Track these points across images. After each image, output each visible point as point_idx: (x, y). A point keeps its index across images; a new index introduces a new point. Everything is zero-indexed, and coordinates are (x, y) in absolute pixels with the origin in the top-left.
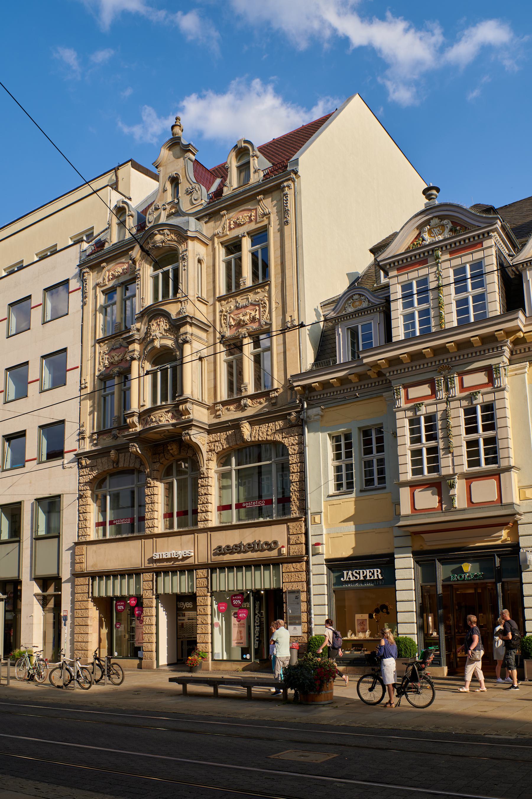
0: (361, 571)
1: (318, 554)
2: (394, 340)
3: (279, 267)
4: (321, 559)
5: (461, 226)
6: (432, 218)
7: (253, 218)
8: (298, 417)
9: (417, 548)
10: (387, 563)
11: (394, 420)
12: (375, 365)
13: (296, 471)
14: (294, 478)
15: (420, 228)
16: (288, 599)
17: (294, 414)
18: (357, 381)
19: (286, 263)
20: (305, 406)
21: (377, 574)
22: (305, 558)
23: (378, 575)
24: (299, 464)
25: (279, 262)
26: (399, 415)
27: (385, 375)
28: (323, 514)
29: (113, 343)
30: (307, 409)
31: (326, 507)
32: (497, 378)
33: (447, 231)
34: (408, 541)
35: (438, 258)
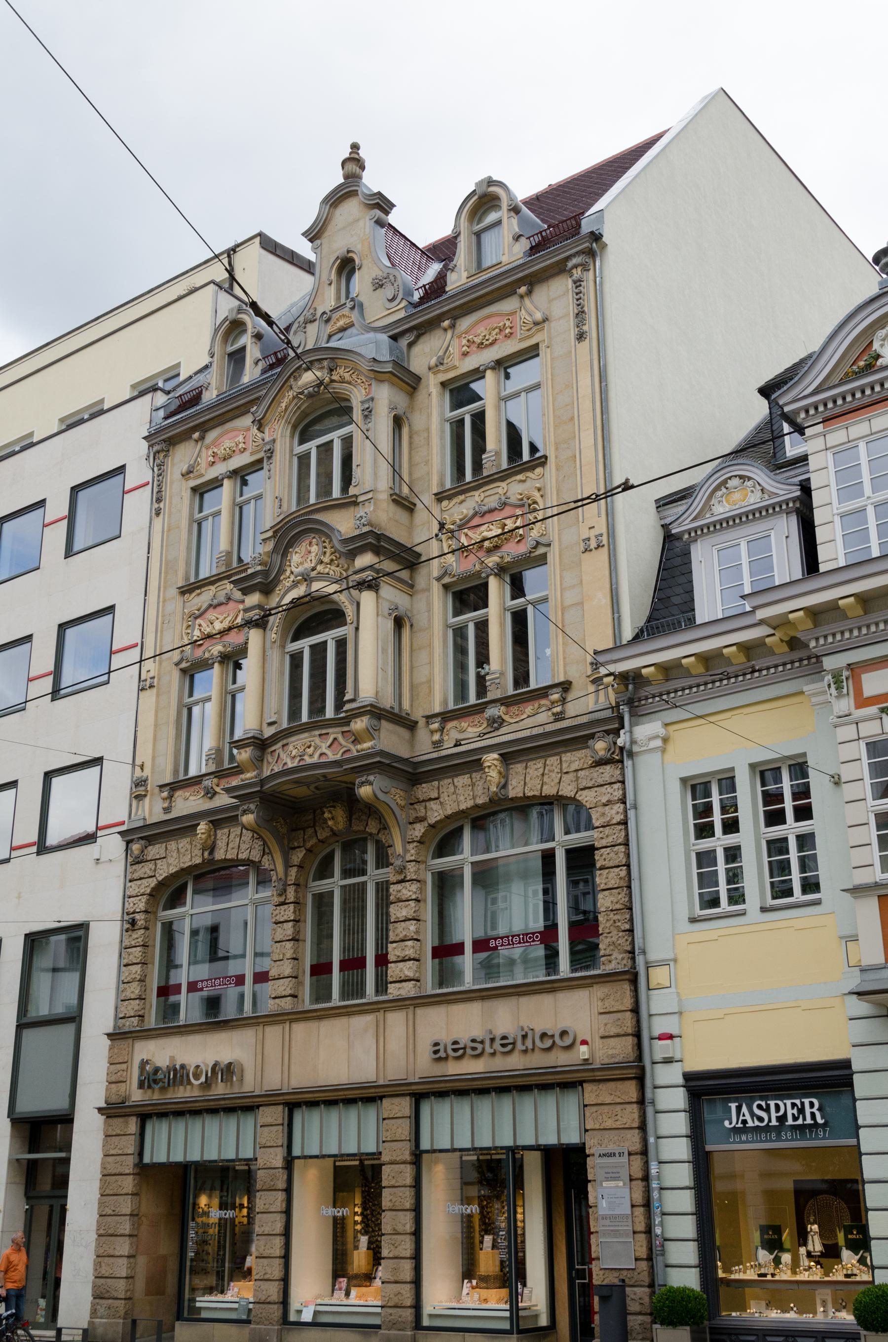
0: (772, 1103)
2: (822, 568)
23: (813, 1115)
29: (211, 593)
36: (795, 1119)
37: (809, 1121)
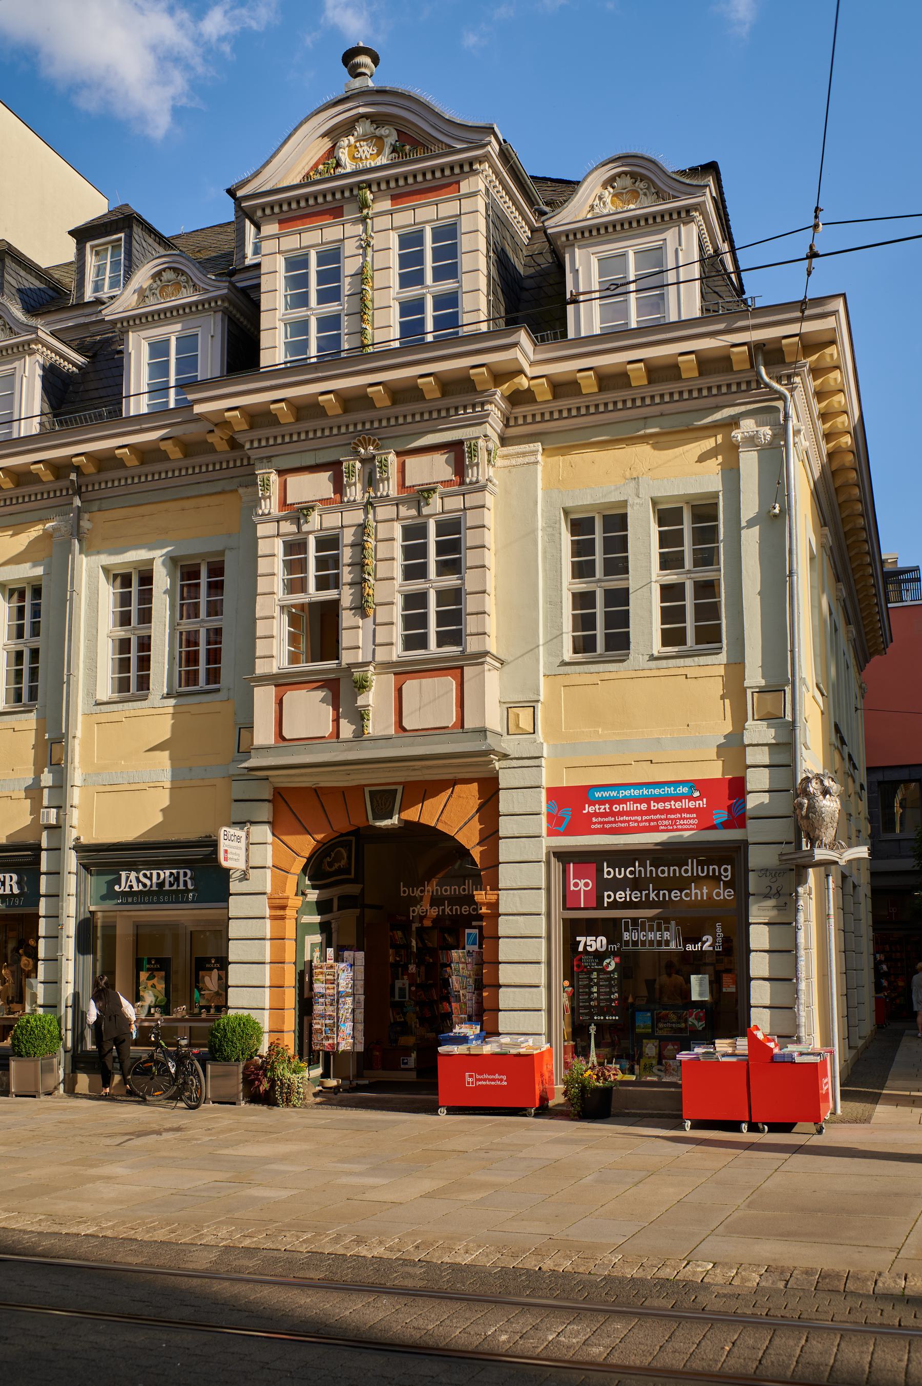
0: (155, 873)
12: (219, 422)
27: (242, 446)
36: (171, 885)
37: (182, 887)
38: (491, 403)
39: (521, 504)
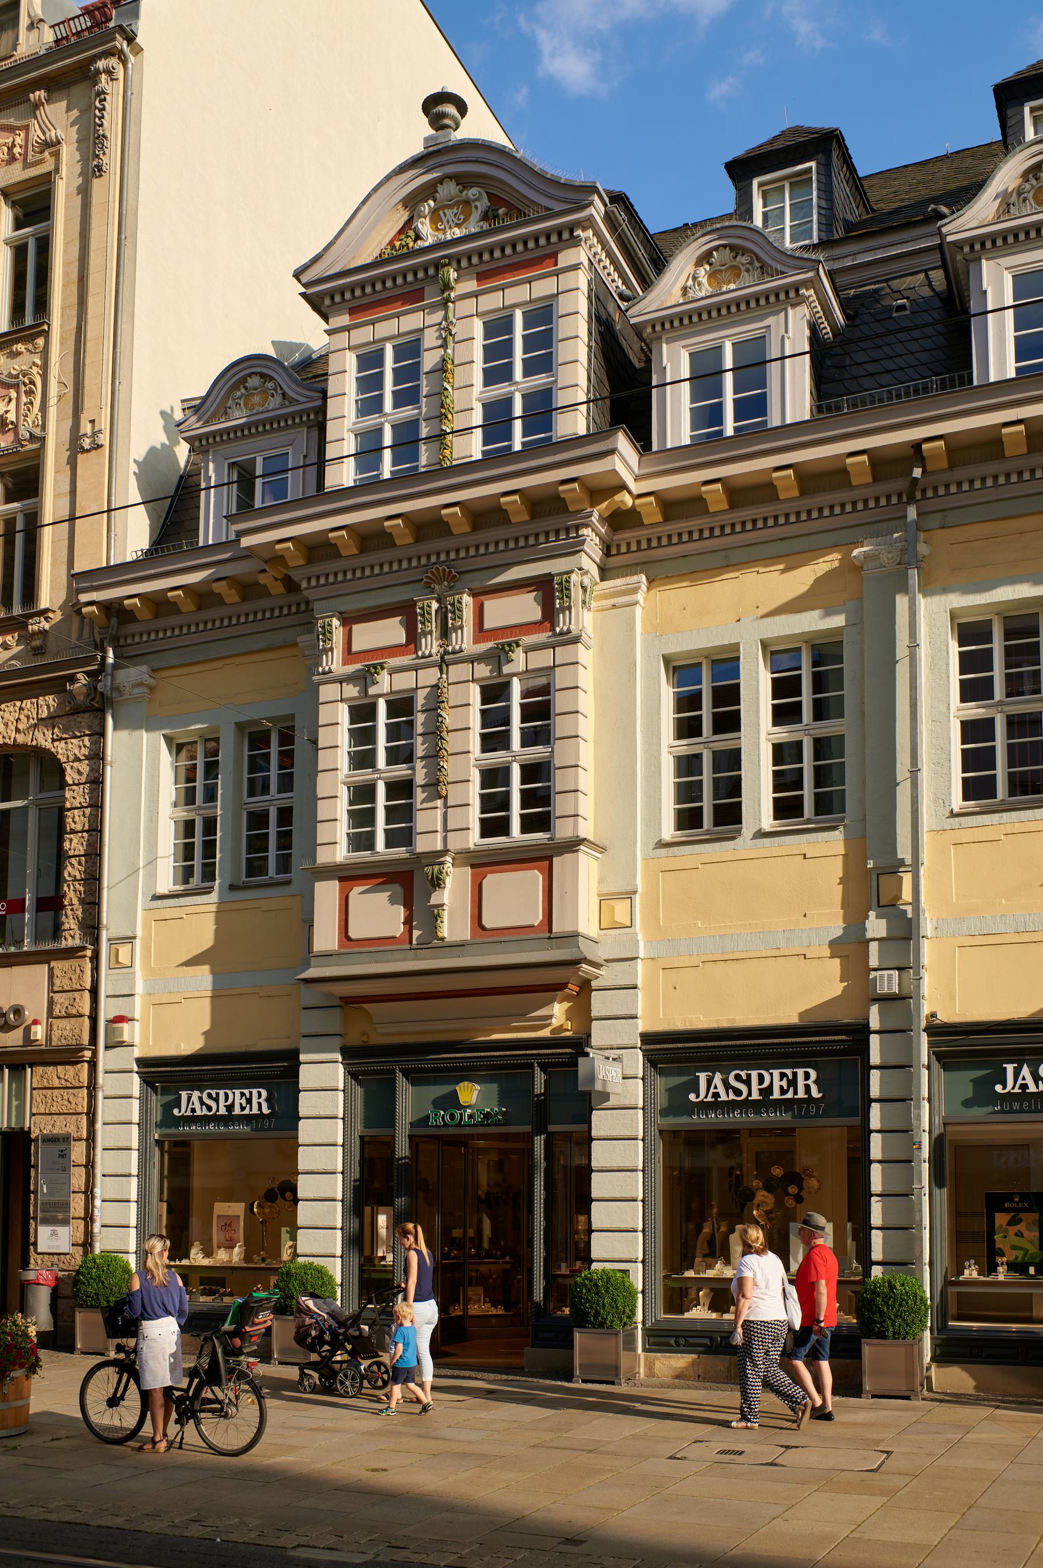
0: (222, 1092)
1: (121, 1044)
3: (74, 288)
4: (126, 1059)
5: (510, 207)
6: (440, 181)
7: (17, 150)
8: (92, 688)
9: (355, 1039)
10: (279, 1072)
11: (314, 704)
13: (79, 827)
14: (75, 845)
15: (412, 202)
16: (39, 1155)
17: (82, 679)
18: (237, 599)
19: (91, 278)
20: (110, 660)
21: (259, 1101)
22: (88, 1054)
24: (88, 811)
25: (75, 276)
26: (328, 692)
28: (138, 942)
30: (116, 666)
31: (146, 926)
32: (563, 610)
33: (476, 216)
34: (332, 1021)
35: (447, 287)
38: (587, 526)
39: (619, 655)
